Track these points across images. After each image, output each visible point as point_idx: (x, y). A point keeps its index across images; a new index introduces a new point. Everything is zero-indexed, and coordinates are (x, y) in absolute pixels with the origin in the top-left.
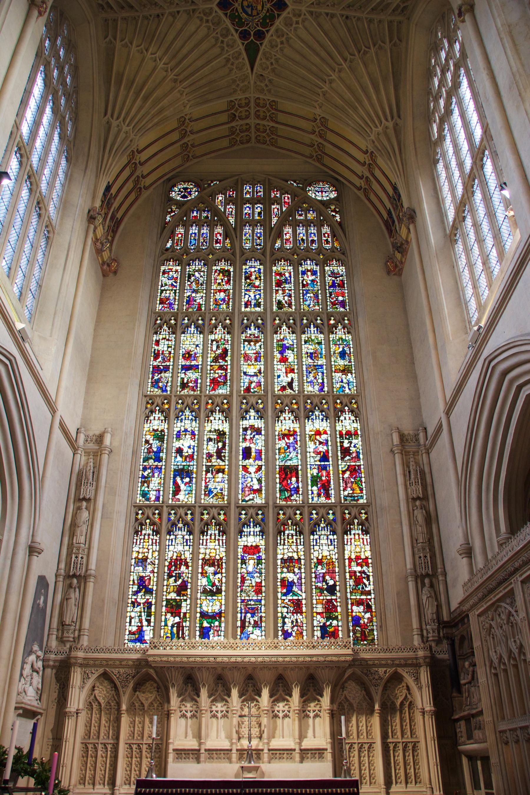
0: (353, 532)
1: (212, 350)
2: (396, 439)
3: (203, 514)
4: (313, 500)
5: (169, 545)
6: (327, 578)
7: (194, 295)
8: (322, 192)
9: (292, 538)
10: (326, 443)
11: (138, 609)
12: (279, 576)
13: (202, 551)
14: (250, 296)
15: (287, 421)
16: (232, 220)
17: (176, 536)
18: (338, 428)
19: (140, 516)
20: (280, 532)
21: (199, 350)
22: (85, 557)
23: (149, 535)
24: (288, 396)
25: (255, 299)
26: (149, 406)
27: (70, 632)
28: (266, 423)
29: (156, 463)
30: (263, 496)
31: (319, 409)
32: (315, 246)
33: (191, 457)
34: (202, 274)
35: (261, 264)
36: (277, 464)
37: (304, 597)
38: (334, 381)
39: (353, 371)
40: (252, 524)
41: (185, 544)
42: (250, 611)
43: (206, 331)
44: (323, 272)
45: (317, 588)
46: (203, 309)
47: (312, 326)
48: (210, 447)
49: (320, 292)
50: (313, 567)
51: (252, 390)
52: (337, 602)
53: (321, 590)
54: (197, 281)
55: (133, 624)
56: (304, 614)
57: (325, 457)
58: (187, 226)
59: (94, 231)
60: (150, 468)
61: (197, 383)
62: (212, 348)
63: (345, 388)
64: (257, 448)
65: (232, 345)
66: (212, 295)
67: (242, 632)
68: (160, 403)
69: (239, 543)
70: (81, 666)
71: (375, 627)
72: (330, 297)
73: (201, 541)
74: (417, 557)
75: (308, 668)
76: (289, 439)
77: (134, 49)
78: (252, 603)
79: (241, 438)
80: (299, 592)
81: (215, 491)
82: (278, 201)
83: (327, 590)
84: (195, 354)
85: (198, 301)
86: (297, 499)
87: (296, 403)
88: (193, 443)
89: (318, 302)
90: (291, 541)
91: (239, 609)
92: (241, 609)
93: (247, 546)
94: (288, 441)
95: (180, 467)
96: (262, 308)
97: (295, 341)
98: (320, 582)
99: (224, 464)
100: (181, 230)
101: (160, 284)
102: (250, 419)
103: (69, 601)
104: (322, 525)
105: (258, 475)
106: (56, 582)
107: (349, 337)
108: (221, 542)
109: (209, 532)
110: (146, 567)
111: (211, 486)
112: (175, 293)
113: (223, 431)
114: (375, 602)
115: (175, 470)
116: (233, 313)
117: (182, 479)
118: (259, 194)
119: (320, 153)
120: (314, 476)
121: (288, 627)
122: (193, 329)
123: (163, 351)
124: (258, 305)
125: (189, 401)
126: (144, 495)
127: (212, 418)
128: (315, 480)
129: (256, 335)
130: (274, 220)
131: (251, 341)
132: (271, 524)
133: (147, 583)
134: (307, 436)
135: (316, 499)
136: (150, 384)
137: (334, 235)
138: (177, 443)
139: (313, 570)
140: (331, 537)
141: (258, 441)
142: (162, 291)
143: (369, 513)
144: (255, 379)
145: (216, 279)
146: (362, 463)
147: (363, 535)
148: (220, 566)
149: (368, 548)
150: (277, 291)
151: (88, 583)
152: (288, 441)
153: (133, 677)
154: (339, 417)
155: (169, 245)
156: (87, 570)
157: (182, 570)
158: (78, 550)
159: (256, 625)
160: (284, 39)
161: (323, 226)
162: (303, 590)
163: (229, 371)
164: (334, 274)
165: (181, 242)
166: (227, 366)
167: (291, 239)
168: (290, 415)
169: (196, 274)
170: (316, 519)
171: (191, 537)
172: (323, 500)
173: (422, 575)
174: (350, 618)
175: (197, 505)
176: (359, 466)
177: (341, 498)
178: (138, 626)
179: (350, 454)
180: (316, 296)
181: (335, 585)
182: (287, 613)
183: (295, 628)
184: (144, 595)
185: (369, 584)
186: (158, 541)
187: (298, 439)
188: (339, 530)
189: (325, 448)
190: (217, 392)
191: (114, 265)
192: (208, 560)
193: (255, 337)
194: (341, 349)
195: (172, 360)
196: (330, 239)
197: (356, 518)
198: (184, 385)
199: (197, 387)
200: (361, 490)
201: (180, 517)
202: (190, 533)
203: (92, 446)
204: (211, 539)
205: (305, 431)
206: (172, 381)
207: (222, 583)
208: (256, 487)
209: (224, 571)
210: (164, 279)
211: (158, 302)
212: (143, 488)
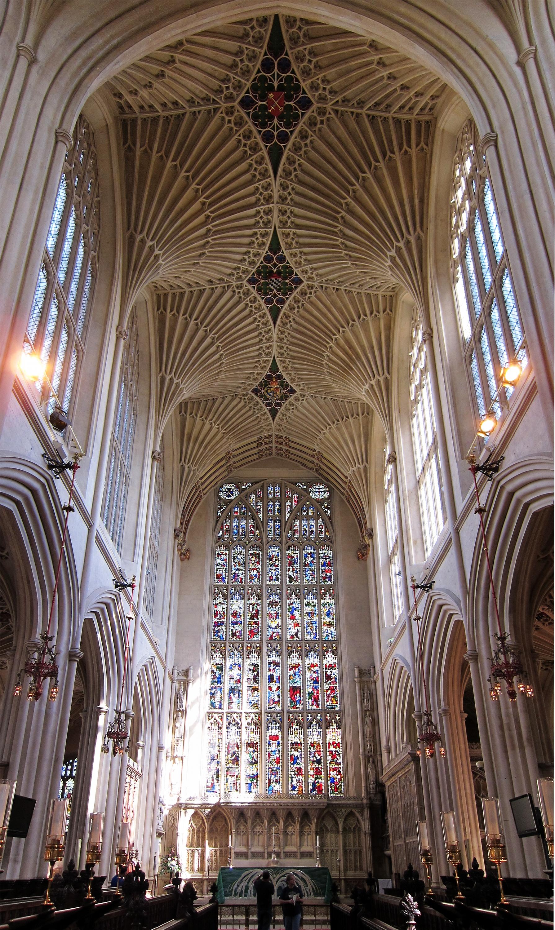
6: (316, 754)
16: (260, 515)
24: (295, 642)
28: (282, 659)
32: (313, 535)
44: (318, 554)
53: (313, 762)
57: (316, 681)
77: (198, 418)
82: (290, 499)
86: (300, 707)
105: (277, 693)
121: (294, 783)
124: (277, 579)
128: (311, 695)
160: (294, 407)
172: (314, 707)
181: (320, 759)
188: (324, 727)
208: (277, 699)
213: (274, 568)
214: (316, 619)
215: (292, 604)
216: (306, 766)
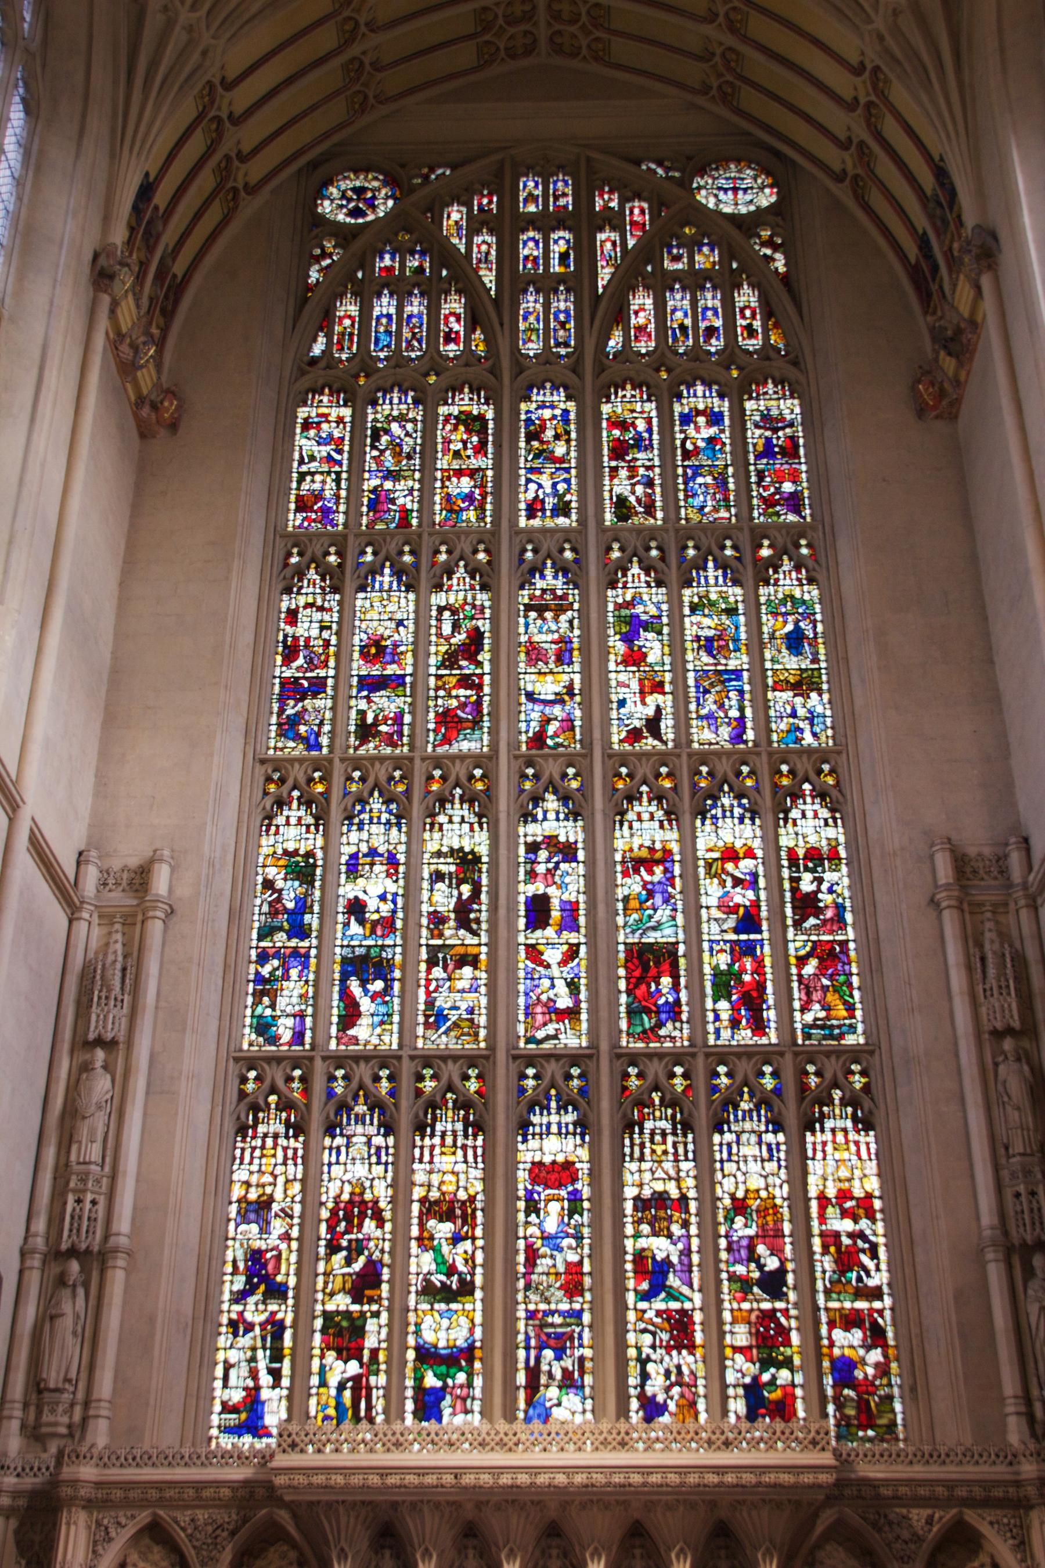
0: (829, 1124)
1: (439, 635)
2: (944, 871)
3: (421, 1078)
4: (718, 1037)
5: (330, 1164)
6: (761, 1249)
7: (388, 485)
8: (735, 190)
9: (664, 1142)
10: (752, 882)
11: (245, 1341)
12: (629, 1244)
13: (420, 1177)
14: (540, 486)
15: (646, 825)
16: (489, 278)
17: (349, 1137)
18: (786, 841)
19: (250, 1086)
20: (630, 1126)
21: (406, 635)
22: (102, 1200)
23: (276, 1136)
25: (555, 493)
26: (272, 788)
27: (60, 1409)
29: (294, 943)
30: (584, 1026)
31: (731, 789)
33: (388, 924)
34: (409, 426)
35: (569, 398)
36: (621, 939)
37: (698, 1303)
38: (772, 713)
39: (825, 687)
40: (553, 1104)
41: (374, 1159)
42: (552, 1342)
43: (424, 584)
45: (733, 1278)
46: (414, 522)
47: (710, 564)
48: (437, 897)
49: (730, 470)
50: (721, 1219)
51: (549, 742)
52: (788, 1317)
53: (744, 1285)
54: (396, 447)
55: (233, 1380)
56: (699, 1353)
57: (749, 921)
58: (366, 297)
59: (112, 311)
60: (277, 955)
61: (402, 724)
62: (439, 628)
63: (802, 731)
64: (565, 897)
65: (495, 620)
66: (438, 484)
67: (529, 1402)
68: (302, 780)
69: (520, 1157)
70: (89, 1505)
71: (896, 1391)
72: (759, 484)
73: (417, 1152)
74: (1009, 1193)
75: (713, 1505)
76: (651, 873)
78: (557, 1320)
79: (522, 870)
80: (685, 1290)
81: (454, 1015)
82: (614, 220)
83: (760, 1283)
84: (396, 645)
85: (400, 501)
87: (669, 775)
88: (392, 887)
89: (726, 499)
90: (659, 1149)
91: (521, 1337)
92: (528, 1338)
93: (541, 1164)
94: (647, 878)
95: (358, 951)
96: (574, 517)
97: (665, 607)
98: (740, 1261)
99: (477, 942)
100: (350, 308)
101: (296, 456)
102: (545, 819)
103: (59, 1322)
104: (745, 1106)
106: (21, 1272)
107: (811, 593)
108: (470, 1152)
109: (439, 1127)
110: (268, 1223)
111: (442, 1001)
112: (338, 481)
113: (472, 852)
114: (893, 1318)
115: (344, 959)
116: (496, 532)
117: (364, 983)
118: (562, 202)
119: (729, 77)
120: (722, 973)
121: (655, 1386)
122: (387, 578)
123: (308, 639)
124: (562, 509)
125: (381, 772)
126: (263, 1027)
127: (442, 819)
128: (723, 984)
129: (559, 593)
130: (605, 275)
131: (547, 608)
132: (605, 1104)
133: (270, 1267)
134: (701, 863)
135: (726, 1034)
136: (274, 728)
137: (768, 311)
138: (349, 887)
139: (722, 1230)
140: (769, 1138)
141: (567, 880)
142: (302, 476)
143: (872, 1073)
144: (557, 711)
145: (447, 441)
146: (851, 935)
147: (858, 1132)
148: (468, 1218)
149: (872, 1167)
150: (614, 470)
151: (110, 1273)
152: (647, 878)
153: (233, 1533)
154: (787, 811)
155: (318, 349)
156: (106, 1237)
157: (365, 1230)
158: (84, 1180)
159: (569, 1382)
161: (739, 286)
162: (696, 1285)
163: (487, 690)
164: (769, 421)
165: (351, 340)
166: (481, 676)
167: (651, 327)
168: (653, 809)
169: (395, 427)
170: (727, 1088)
171: (391, 1140)
172: (745, 1036)
173: (1024, 1244)
174: (826, 1364)
175: (405, 1053)
176: (844, 944)
177: (793, 1030)
178: (245, 1389)
179: (818, 912)
180: (721, 482)
181: (782, 1271)
182: (653, 1347)
183: (676, 1390)
184: (264, 1303)
185: (878, 1269)
186: (300, 1153)
187: (677, 871)
188: (791, 1118)
189: (750, 894)
190: (455, 748)
191: (170, 406)
192: (437, 1202)
193: (556, 597)
194: (790, 627)
195: (332, 663)
196: (757, 324)
197: (836, 1086)
198: (366, 731)
199: (401, 734)
200: (850, 1009)
201: (360, 1088)
202: (388, 1128)
203: (119, 898)
204: (443, 1145)
205: (695, 850)
206: (333, 721)
207: (474, 1267)
208: (564, 1002)
209: (479, 1232)
210: (305, 443)
211: (292, 506)
212: (259, 1010)
213: (550, 468)
214: (738, 661)
215: (629, 604)
216: (714, 1305)
